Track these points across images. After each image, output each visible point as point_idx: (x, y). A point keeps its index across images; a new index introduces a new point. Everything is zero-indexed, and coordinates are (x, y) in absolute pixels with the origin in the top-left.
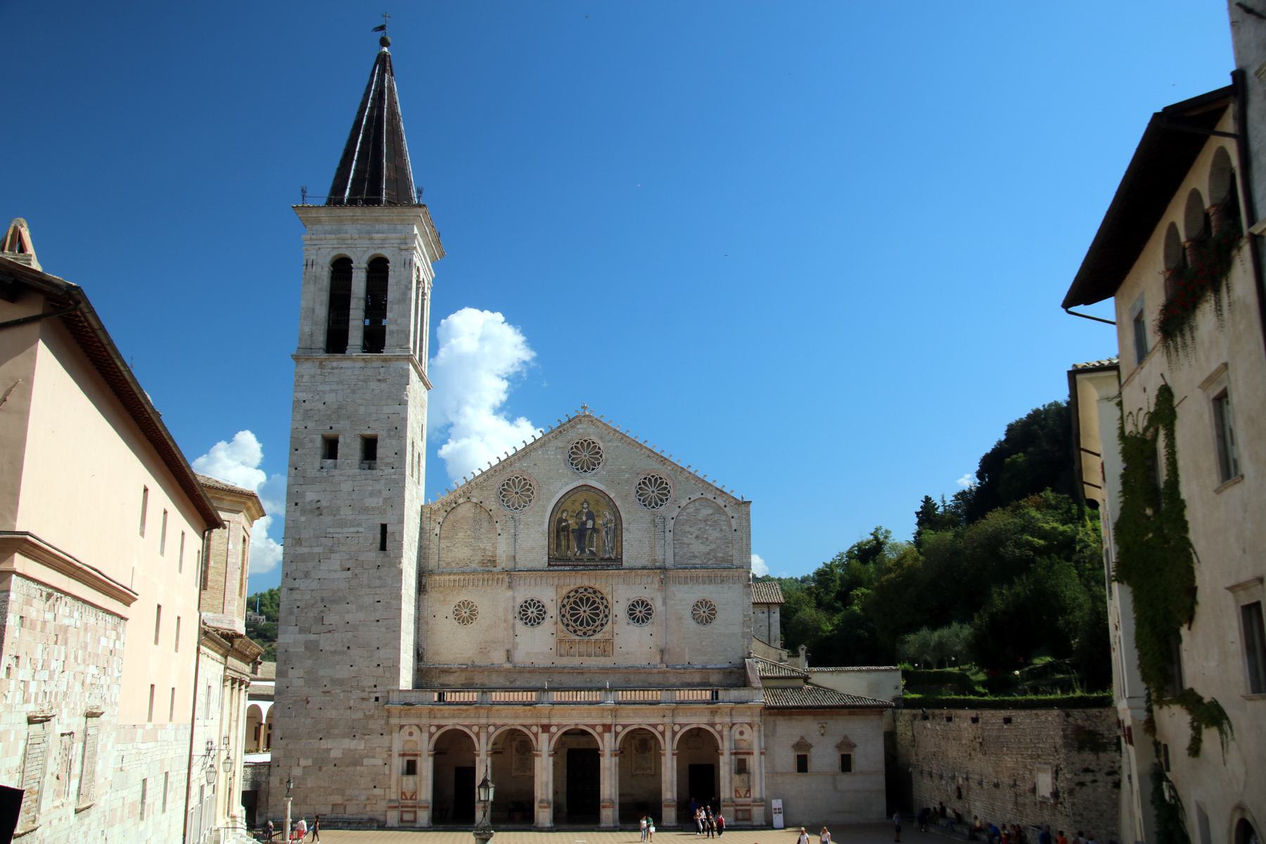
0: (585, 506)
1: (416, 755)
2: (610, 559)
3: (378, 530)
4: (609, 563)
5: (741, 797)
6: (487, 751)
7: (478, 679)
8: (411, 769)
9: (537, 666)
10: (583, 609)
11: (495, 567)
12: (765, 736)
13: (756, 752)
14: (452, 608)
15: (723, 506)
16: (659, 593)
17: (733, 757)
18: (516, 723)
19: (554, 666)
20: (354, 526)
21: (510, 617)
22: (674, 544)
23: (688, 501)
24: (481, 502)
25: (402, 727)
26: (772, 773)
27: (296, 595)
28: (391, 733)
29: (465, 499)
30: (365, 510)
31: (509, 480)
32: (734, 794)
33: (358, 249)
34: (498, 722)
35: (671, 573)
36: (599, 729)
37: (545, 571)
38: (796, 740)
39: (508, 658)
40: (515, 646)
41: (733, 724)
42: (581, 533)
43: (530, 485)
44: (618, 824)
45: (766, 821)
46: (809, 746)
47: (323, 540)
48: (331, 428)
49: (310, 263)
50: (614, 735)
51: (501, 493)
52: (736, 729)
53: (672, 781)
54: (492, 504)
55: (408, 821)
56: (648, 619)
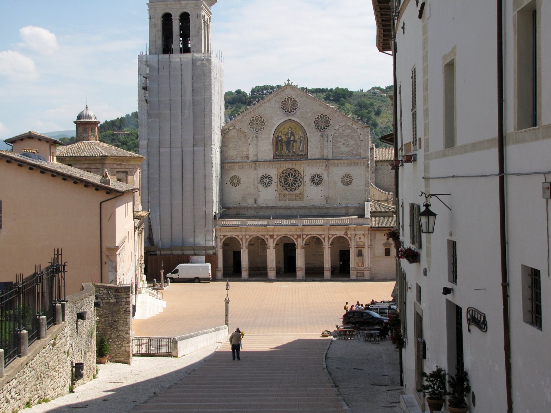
0: (290, 129)
2: (302, 155)
4: (301, 157)
5: (359, 266)
6: (246, 246)
7: (242, 212)
9: (269, 205)
10: (290, 179)
11: (248, 159)
12: (371, 240)
13: (366, 247)
14: (229, 179)
15: (356, 129)
16: (325, 171)
17: (356, 249)
18: (258, 234)
19: (277, 205)
21: (256, 183)
22: (332, 147)
23: (339, 127)
24: (240, 129)
26: (374, 256)
29: (233, 127)
31: (253, 117)
32: (356, 266)
33: (175, 9)
34: (251, 234)
35: (331, 162)
36: (295, 237)
37: (272, 161)
39: (256, 202)
41: (356, 235)
43: (263, 120)
45: (370, 277)
49: (152, 17)
50: (302, 240)
51: (250, 124)
52: (357, 237)
53: (328, 259)
54: (246, 129)
56: (320, 183)
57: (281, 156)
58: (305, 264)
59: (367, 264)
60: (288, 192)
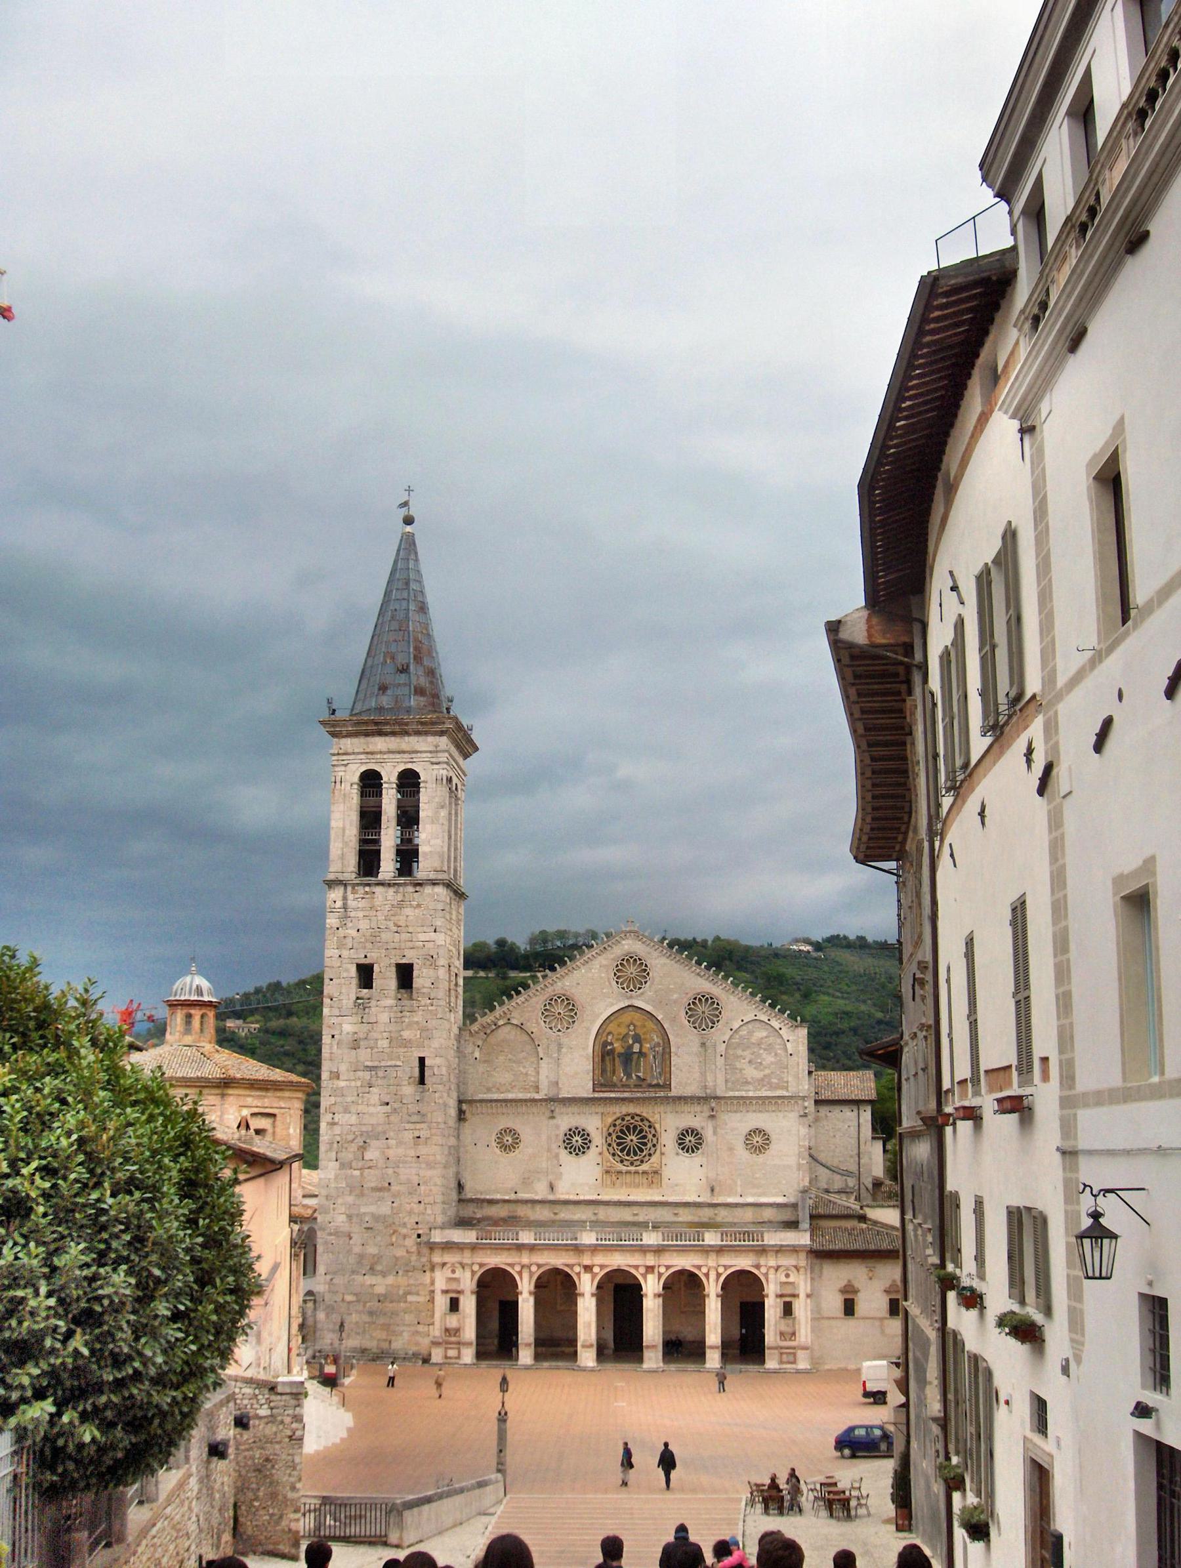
0: (632, 1028)
1: (459, 1292)
2: (658, 1085)
3: (417, 1063)
5: (786, 1340)
8: (454, 1305)
13: (802, 1296)
14: (494, 1137)
17: (778, 1300)
20: (392, 1060)
21: (554, 1146)
25: (444, 1264)
26: (818, 1318)
27: (337, 1129)
28: (432, 1269)
30: (406, 1044)
34: (541, 1261)
36: (642, 1270)
38: (843, 1283)
40: (559, 1176)
42: (628, 1058)
44: (661, 1364)
46: (856, 1291)
47: (360, 1074)
48: (366, 957)
49: (338, 780)
55: (450, 1358)
56: (698, 1149)
57: (611, 1086)
58: (664, 1333)
59: (804, 1335)
60: (624, 1168)
